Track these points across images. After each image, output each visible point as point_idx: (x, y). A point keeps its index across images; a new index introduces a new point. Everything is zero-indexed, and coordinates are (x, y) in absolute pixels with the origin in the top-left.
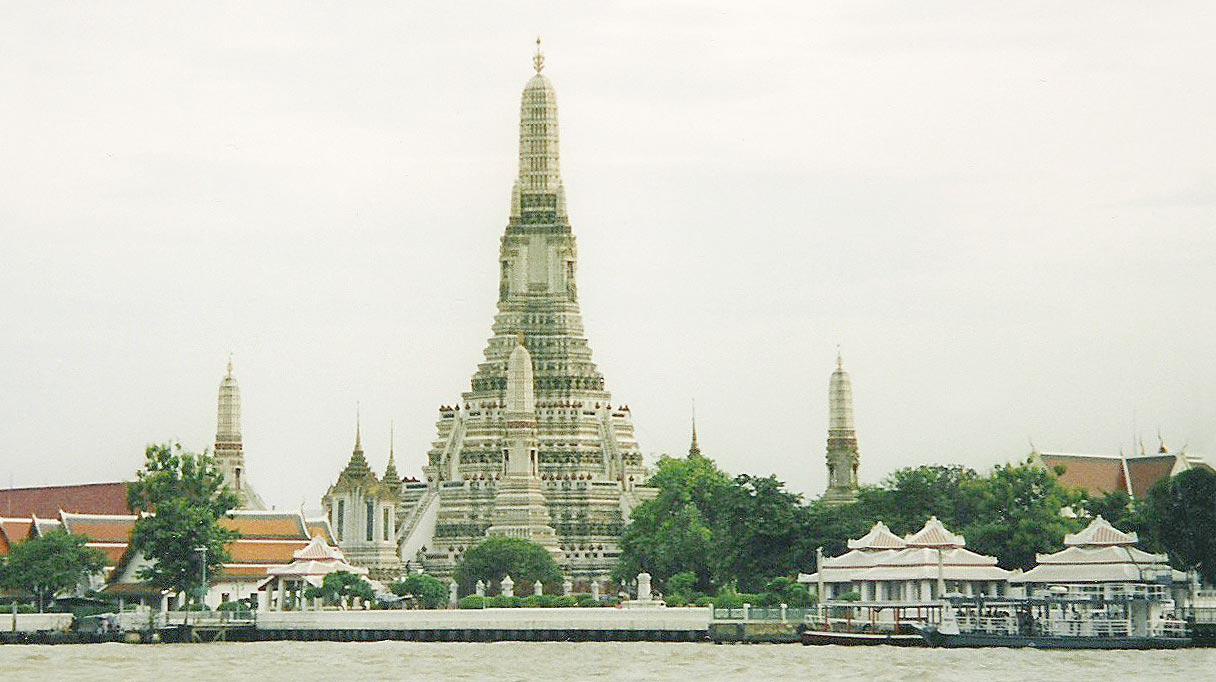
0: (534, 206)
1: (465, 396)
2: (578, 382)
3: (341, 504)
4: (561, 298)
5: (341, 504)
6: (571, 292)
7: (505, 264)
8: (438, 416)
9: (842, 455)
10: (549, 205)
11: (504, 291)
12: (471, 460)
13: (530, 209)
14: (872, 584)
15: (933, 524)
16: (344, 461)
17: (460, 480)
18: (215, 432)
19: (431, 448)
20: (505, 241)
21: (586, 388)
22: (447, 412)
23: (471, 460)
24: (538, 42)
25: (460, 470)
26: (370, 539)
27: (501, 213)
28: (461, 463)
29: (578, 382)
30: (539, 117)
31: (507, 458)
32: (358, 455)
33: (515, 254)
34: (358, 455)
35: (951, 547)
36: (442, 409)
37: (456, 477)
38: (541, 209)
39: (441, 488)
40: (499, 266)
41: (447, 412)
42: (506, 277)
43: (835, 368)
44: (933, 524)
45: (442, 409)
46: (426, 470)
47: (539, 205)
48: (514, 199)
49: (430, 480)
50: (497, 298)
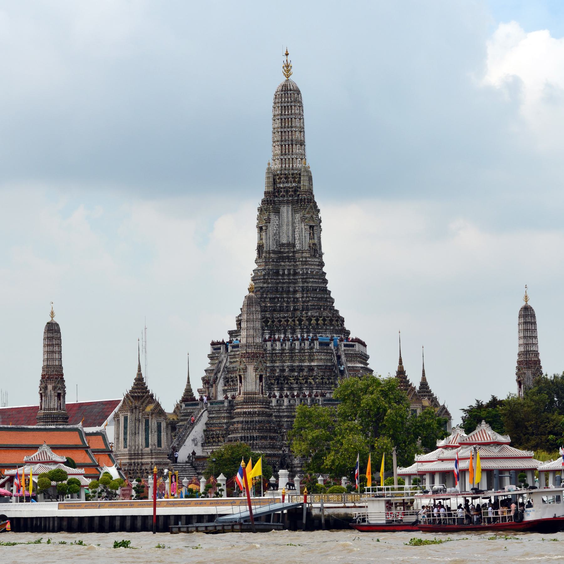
0: (283, 183)
1: (231, 333)
2: (317, 320)
3: (126, 419)
4: (304, 255)
6: (316, 250)
7: (261, 229)
9: (529, 373)
10: (294, 182)
11: (260, 248)
12: (232, 384)
13: (281, 186)
14: (432, 474)
15: (484, 426)
19: (204, 374)
21: (324, 324)
23: (232, 384)
24: (287, 55)
25: (225, 391)
26: (147, 446)
28: (225, 385)
29: (317, 320)
30: (286, 113)
31: (241, 382)
32: (140, 381)
33: (268, 221)
34: (140, 381)
35: (498, 444)
36: (213, 344)
37: (221, 397)
38: (289, 185)
40: (256, 230)
42: (262, 239)
43: (523, 304)
44: (484, 426)
45: (213, 344)
47: (287, 182)
49: (202, 399)
50: (255, 255)
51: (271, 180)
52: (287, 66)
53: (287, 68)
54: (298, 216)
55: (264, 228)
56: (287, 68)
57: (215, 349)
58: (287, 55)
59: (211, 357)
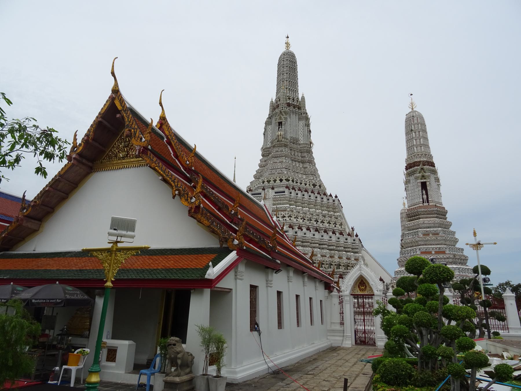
24: (288, 37)
33: (286, 119)
54: (302, 123)
55: (283, 123)
56: (287, 44)
58: (288, 37)
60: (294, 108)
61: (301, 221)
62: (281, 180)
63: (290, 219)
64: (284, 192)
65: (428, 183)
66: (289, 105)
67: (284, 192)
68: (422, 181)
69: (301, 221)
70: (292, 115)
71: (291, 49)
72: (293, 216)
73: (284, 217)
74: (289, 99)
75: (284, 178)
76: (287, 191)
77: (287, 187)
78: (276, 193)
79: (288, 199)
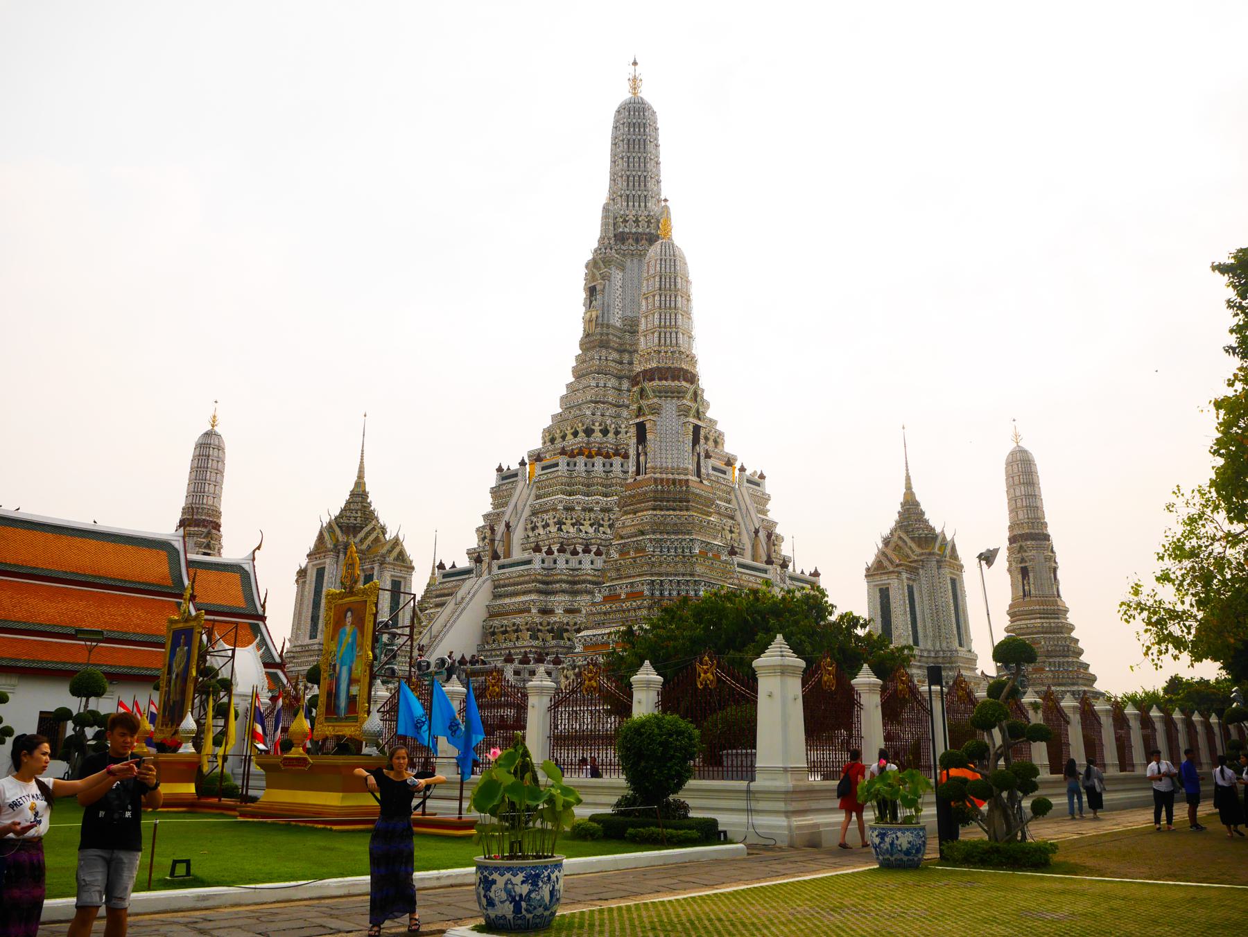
3: (320, 573)
5: (320, 573)
7: (592, 291)
8: (492, 480)
16: (335, 504)
17: (526, 556)
18: (182, 503)
20: (593, 265)
22: (506, 476)
24: (635, 63)
27: (587, 235)
32: (359, 497)
34: (359, 497)
39: (495, 570)
41: (506, 476)
46: (469, 553)
48: (605, 217)
51: (611, 221)
52: (635, 80)
53: (635, 82)
55: (598, 288)
56: (635, 82)
57: (504, 478)
58: (635, 63)
59: (495, 492)
60: (637, 241)
61: (591, 530)
62: (575, 434)
63: (560, 529)
64: (556, 465)
65: (648, 425)
66: (621, 238)
67: (556, 465)
68: (638, 420)
69: (591, 530)
70: (628, 263)
71: (646, 94)
72: (569, 522)
73: (547, 525)
74: (625, 221)
75: (580, 428)
76: (562, 461)
77: (563, 452)
78: (543, 469)
79: (564, 480)
